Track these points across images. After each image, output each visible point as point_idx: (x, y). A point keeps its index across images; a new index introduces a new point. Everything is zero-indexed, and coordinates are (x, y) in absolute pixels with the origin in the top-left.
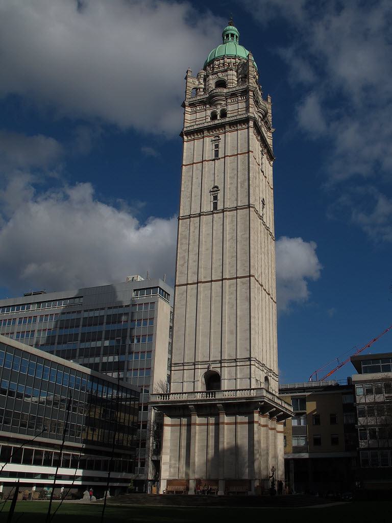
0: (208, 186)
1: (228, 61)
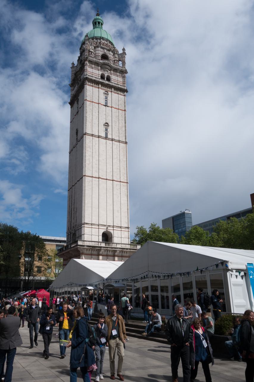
0: (102, 122)
1: (103, 41)
